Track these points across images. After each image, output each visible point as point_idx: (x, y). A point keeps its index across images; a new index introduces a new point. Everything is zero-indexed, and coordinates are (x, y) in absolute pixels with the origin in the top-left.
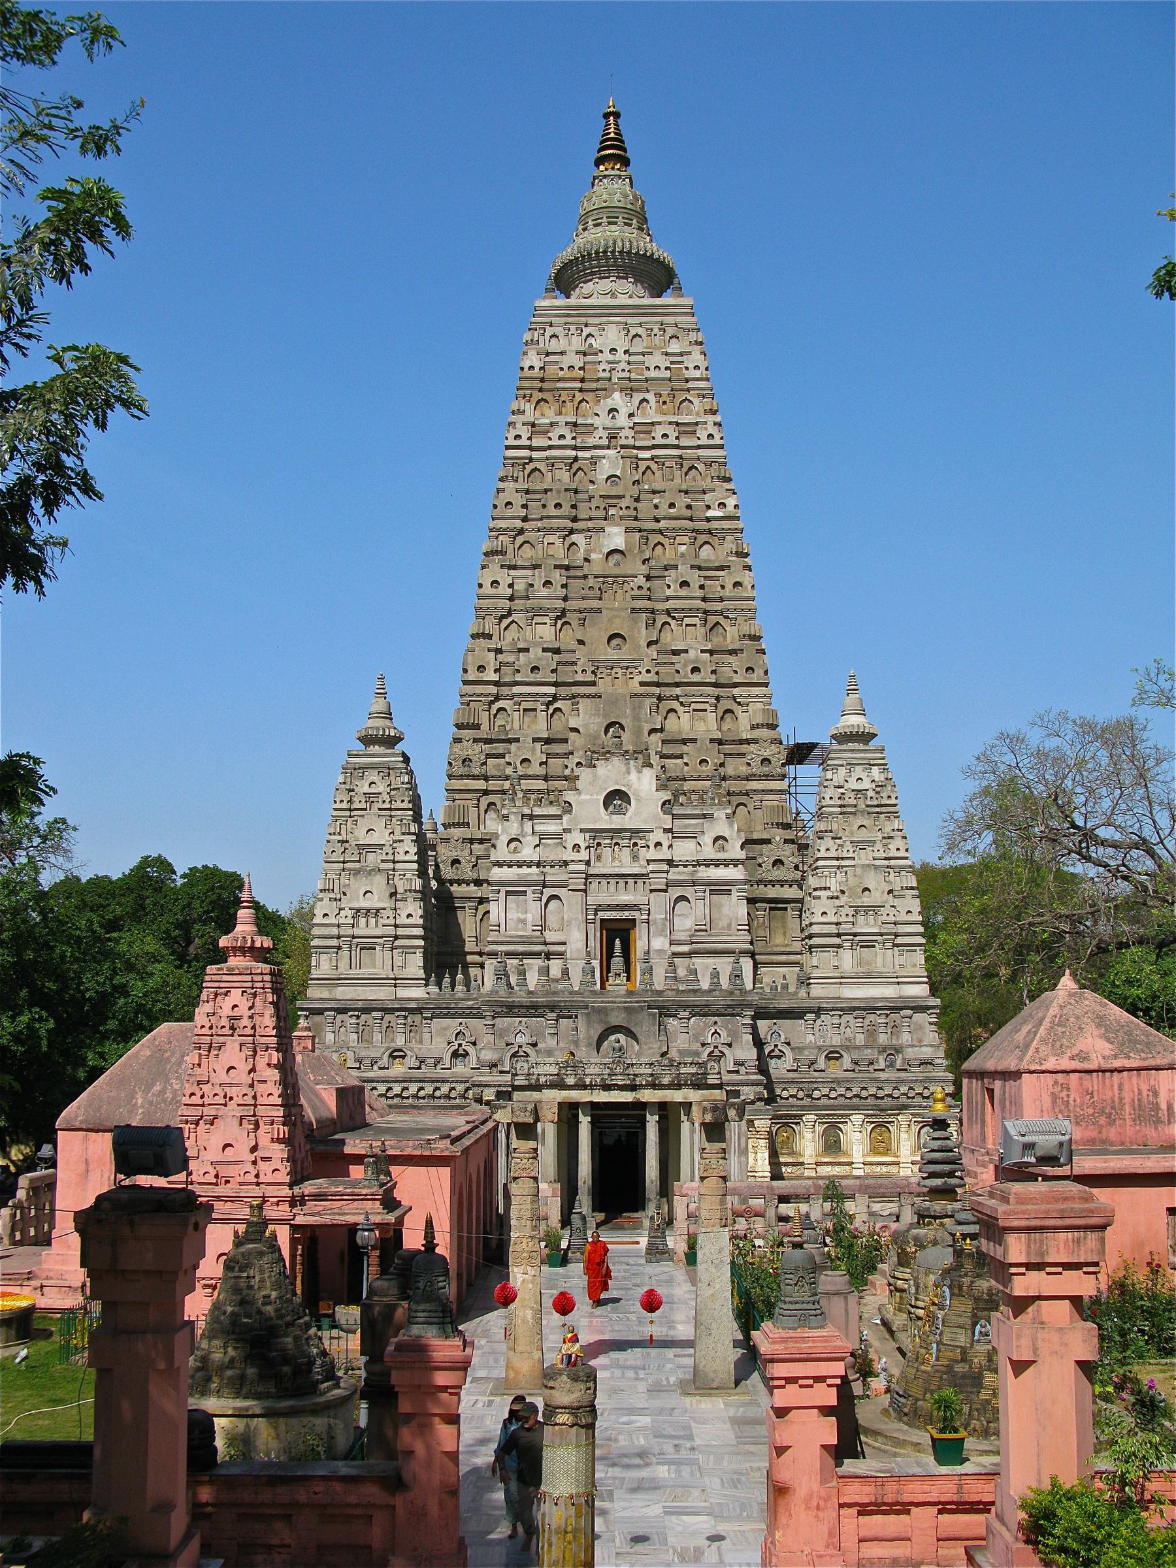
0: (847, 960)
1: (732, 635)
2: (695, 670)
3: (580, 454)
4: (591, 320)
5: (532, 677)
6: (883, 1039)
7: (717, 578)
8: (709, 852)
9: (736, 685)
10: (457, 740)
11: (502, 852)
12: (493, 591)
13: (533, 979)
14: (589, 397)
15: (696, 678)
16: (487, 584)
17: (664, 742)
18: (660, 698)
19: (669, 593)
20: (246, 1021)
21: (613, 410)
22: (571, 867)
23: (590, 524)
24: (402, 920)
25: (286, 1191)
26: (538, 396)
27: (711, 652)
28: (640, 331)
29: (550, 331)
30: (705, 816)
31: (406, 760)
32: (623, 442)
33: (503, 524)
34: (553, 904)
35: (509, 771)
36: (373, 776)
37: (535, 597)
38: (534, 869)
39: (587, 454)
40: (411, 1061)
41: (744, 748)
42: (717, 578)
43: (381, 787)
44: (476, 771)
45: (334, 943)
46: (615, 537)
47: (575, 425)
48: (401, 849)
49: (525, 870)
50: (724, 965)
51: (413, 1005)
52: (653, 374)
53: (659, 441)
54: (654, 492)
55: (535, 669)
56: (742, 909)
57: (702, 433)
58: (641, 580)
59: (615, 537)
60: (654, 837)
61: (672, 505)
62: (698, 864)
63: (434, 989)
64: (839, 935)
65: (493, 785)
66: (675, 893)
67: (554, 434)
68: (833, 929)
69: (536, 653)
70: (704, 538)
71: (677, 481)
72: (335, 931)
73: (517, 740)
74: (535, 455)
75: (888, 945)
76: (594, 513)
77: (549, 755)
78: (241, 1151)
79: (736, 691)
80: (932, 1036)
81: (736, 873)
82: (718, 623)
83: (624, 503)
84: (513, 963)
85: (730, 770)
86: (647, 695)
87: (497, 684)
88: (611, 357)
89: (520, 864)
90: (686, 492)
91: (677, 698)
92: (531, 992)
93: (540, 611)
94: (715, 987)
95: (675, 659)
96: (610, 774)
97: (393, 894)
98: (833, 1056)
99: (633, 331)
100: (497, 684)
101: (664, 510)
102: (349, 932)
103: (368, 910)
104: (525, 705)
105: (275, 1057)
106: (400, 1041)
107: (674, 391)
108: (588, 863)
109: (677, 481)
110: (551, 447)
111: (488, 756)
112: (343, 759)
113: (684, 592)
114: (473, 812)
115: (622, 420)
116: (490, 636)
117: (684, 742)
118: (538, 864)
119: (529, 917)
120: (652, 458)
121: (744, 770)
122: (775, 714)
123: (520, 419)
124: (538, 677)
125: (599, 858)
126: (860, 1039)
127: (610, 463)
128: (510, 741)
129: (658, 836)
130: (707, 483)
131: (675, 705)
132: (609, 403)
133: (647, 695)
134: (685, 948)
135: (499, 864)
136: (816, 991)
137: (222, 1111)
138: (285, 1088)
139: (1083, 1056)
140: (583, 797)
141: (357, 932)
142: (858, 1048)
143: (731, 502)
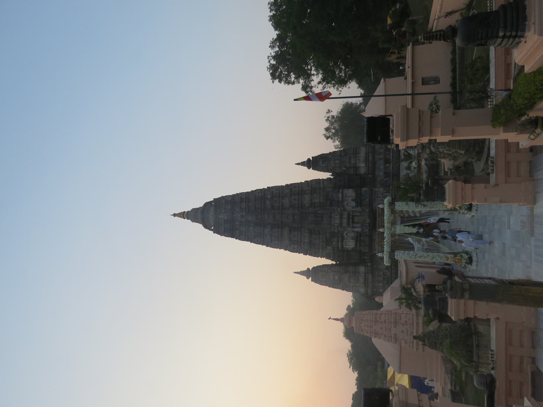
27: (291, 195)
34: (349, 234)
40: (387, 271)
52: (230, 207)
53: (244, 207)
55: (294, 236)
56: (350, 190)
89: (338, 242)
106: (382, 273)
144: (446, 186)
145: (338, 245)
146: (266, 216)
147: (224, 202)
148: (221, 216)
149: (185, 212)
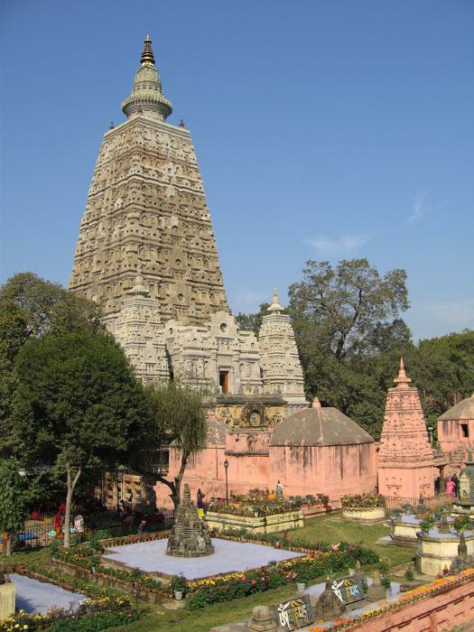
1: (211, 266)
5: (152, 272)
15: (203, 281)
16: (134, 231)
21: (169, 169)
46: (175, 221)
49: (197, 351)
58: (183, 239)
104: (151, 283)
107: (187, 166)
108: (217, 350)
115: (172, 174)
124: (155, 272)
127: (170, 191)
130: (200, 206)
143: (209, 215)
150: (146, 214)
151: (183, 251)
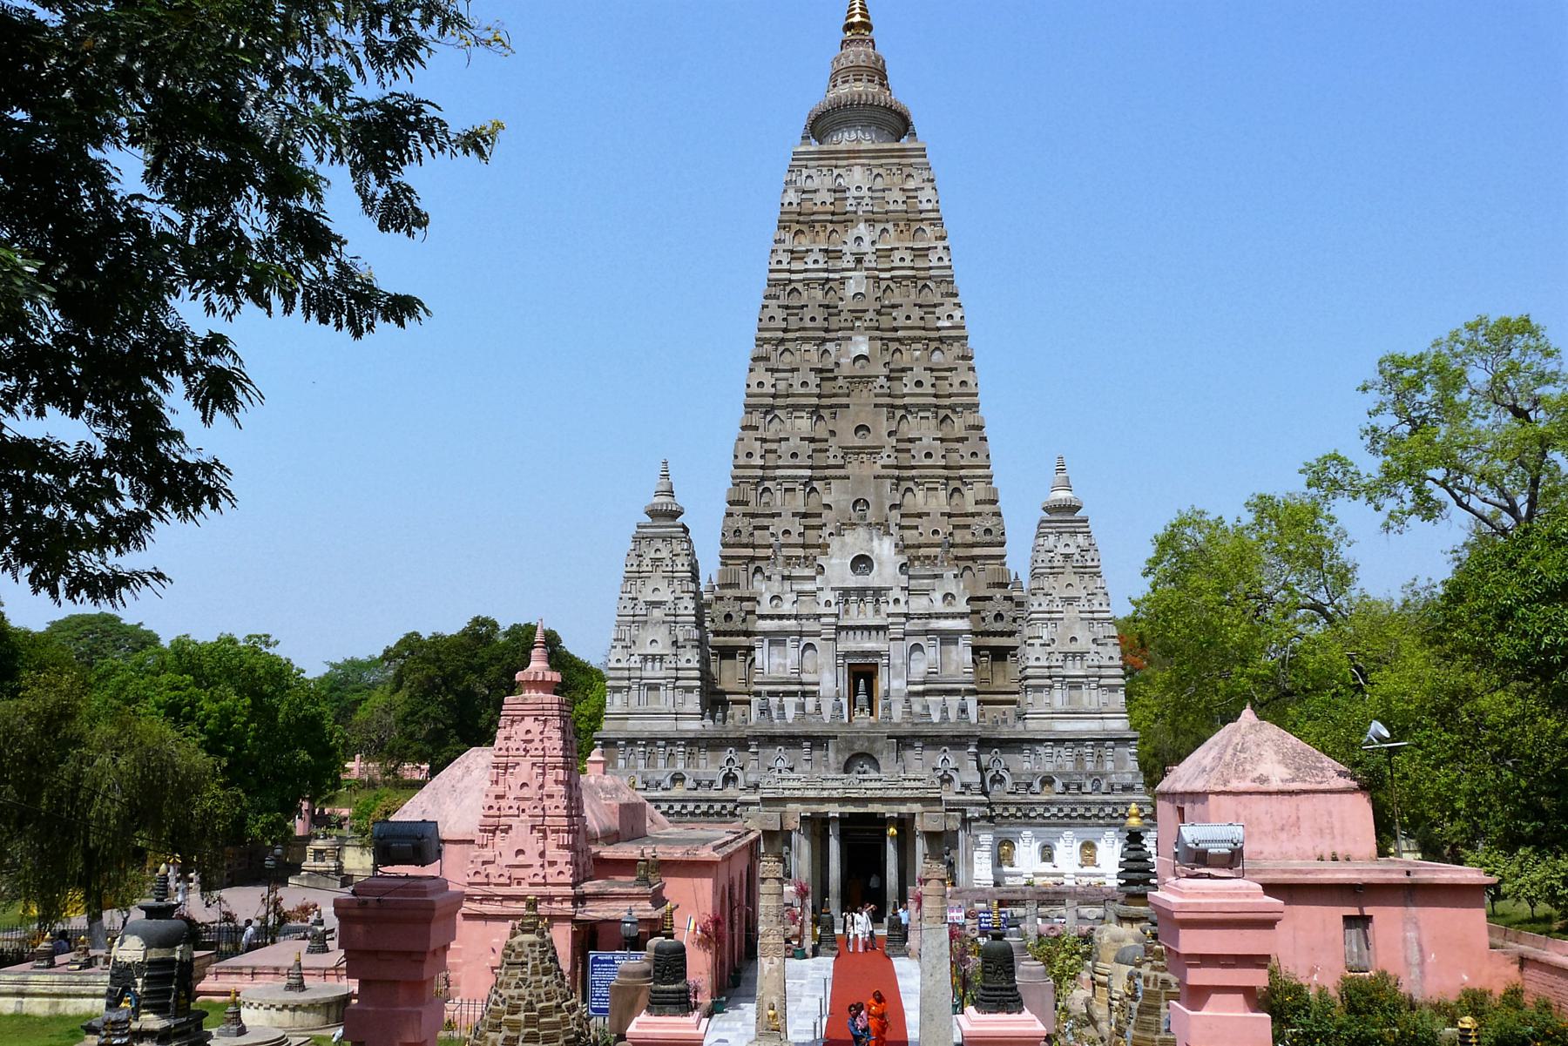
0: (1058, 698)
2: (929, 455)
3: (831, 276)
4: (840, 163)
5: (792, 462)
6: (1090, 766)
7: (946, 378)
8: (939, 607)
9: (962, 467)
10: (729, 515)
11: (765, 608)
12: (759, 391)
13: (790, 713)
14: (838, 227)
15: (929, 462)
17: (902, 516)
18: (899, 479)
19: (906, 391)
20: (537, 744)
22: (823, 620)
23: (840, 334)
24: (682, 664)
25: (569, 891)
26: (796, 227)
27: (942, 440)
28: (880, 171)
29: (805, 172)
30: (936, 576)
31: (686, 531)
32: (866, 265)
33: (767, 335)
34: (808, 653)
35: (772, 540)
36: (659, 544)
37: (794, 395)
38: (793, 622)
39: (837, 276)
40: (690, 783)
41: (969, 520)
42: (946, 378)
43: (665, 554)
44: (745, 540)
45: (625, 683)
46: (861, 345)
47: (826, 251)
48: (681, 606)
49: (785, 622)
50: (953, 702)
51: (691, 735)
52: (892, 207)
53: (897, 263)
54: (894, 306)
56: (968, 656)
57: (933, 256)
58: (882, 380)
59: (861, 345)
60: (893, 595)
61: (908, 318)
62: (930, 616)
63: (708, 722)
64: (1050, 677)
65: (760, 552)
66: (912, 641)
67: (810, 260)
68: (1046, 672)
69: (794, 443)
70: (933, 345)
71: (913, 297)
72: (626, 674)
73: (779, 515)
74: (794, 277)
75: (1093, 685)
76: (843, 325)
77: (806, 527)
78: (531, 857)
79: (962, 472)
80: (1133, 765)
81: (963, 624)
82: (947, 416)
83: (867, 316)
84: (774, 701)
85: (958, 540)
86: (888, 477)
87: (762, 467)
88: (857, 194)
89: (781, 617)
90: (920, 306)
91: (912, 478)
92: (788, 725)
93: (796, 407)
94: (945, 719)
95: (909, 446)
96: (856, 542)
97: (675, 643)
98: (1047, 781)
99: (875, 171)
100: (762, 467)
101: (901, 322)
102: (638, 674)
103: (654, 658)
104: (786, 485)
105: (561, 774)
106: (680, 766)
108: (837, 616)
109: (913, 297)
110: (806, 271)
111: (756, 528)
112: (633, 530)
113: (918, 390)
114: (743, 575)
115: (866, 247)
116: (756, 428)
117: (920, 515)
118: (796, 617)
119: (789, 662)
120: (892, 278)
121: (969, 539)
122: (995, 490)
123: (781, 247)
124: (797, 462)
125: (847, 612)
126: (1069, 767)
127: (856, 283)
128: (773, 516)
129: (896, 593)
131: (911, 484)
132: (855, 232)
133: (888, 477)
134: (920, 688)
135: (762, 617)
136: (1031, 725)
137: (514, 822)
138: (570, 799)
139: (1263, 779)
140: (833, 561)
141: (644, 674)
142: (1068, 774)
143: (957, 314)
144: (1027, 1014)
145: (771, 617)
146: (864, 349)
147: (911, 184)
148: (857, 170)
149: (869, 27)
150: (789, 345)
151: (876, 406)
